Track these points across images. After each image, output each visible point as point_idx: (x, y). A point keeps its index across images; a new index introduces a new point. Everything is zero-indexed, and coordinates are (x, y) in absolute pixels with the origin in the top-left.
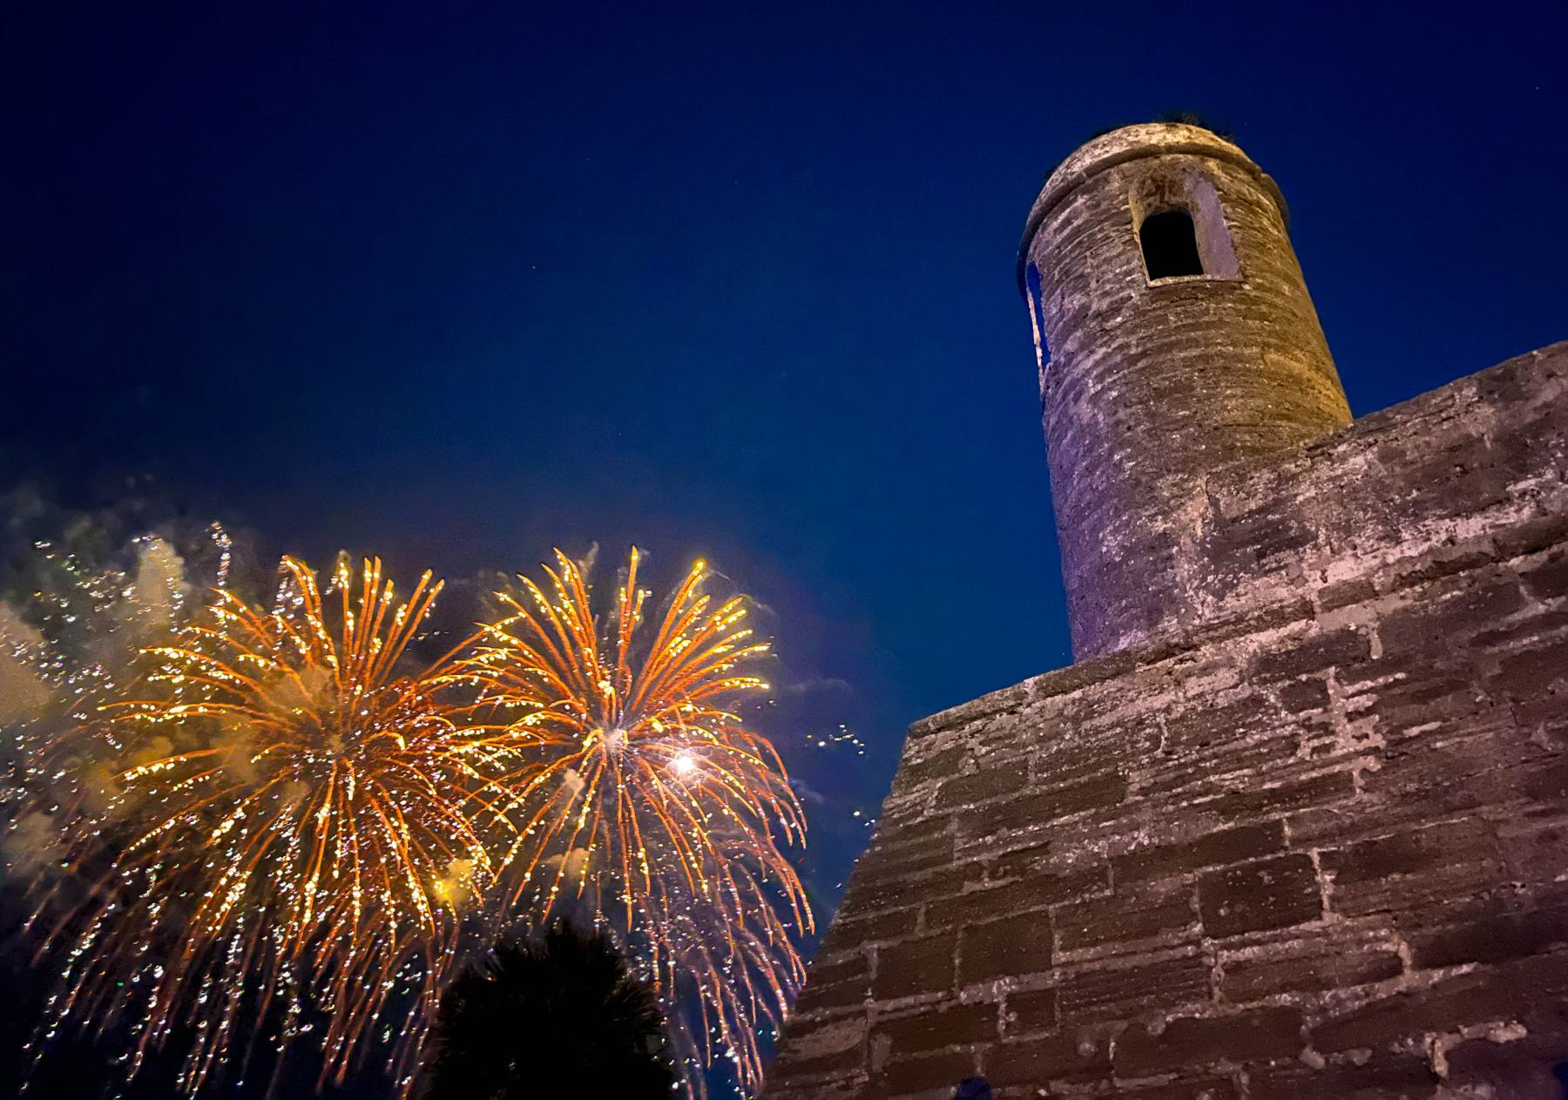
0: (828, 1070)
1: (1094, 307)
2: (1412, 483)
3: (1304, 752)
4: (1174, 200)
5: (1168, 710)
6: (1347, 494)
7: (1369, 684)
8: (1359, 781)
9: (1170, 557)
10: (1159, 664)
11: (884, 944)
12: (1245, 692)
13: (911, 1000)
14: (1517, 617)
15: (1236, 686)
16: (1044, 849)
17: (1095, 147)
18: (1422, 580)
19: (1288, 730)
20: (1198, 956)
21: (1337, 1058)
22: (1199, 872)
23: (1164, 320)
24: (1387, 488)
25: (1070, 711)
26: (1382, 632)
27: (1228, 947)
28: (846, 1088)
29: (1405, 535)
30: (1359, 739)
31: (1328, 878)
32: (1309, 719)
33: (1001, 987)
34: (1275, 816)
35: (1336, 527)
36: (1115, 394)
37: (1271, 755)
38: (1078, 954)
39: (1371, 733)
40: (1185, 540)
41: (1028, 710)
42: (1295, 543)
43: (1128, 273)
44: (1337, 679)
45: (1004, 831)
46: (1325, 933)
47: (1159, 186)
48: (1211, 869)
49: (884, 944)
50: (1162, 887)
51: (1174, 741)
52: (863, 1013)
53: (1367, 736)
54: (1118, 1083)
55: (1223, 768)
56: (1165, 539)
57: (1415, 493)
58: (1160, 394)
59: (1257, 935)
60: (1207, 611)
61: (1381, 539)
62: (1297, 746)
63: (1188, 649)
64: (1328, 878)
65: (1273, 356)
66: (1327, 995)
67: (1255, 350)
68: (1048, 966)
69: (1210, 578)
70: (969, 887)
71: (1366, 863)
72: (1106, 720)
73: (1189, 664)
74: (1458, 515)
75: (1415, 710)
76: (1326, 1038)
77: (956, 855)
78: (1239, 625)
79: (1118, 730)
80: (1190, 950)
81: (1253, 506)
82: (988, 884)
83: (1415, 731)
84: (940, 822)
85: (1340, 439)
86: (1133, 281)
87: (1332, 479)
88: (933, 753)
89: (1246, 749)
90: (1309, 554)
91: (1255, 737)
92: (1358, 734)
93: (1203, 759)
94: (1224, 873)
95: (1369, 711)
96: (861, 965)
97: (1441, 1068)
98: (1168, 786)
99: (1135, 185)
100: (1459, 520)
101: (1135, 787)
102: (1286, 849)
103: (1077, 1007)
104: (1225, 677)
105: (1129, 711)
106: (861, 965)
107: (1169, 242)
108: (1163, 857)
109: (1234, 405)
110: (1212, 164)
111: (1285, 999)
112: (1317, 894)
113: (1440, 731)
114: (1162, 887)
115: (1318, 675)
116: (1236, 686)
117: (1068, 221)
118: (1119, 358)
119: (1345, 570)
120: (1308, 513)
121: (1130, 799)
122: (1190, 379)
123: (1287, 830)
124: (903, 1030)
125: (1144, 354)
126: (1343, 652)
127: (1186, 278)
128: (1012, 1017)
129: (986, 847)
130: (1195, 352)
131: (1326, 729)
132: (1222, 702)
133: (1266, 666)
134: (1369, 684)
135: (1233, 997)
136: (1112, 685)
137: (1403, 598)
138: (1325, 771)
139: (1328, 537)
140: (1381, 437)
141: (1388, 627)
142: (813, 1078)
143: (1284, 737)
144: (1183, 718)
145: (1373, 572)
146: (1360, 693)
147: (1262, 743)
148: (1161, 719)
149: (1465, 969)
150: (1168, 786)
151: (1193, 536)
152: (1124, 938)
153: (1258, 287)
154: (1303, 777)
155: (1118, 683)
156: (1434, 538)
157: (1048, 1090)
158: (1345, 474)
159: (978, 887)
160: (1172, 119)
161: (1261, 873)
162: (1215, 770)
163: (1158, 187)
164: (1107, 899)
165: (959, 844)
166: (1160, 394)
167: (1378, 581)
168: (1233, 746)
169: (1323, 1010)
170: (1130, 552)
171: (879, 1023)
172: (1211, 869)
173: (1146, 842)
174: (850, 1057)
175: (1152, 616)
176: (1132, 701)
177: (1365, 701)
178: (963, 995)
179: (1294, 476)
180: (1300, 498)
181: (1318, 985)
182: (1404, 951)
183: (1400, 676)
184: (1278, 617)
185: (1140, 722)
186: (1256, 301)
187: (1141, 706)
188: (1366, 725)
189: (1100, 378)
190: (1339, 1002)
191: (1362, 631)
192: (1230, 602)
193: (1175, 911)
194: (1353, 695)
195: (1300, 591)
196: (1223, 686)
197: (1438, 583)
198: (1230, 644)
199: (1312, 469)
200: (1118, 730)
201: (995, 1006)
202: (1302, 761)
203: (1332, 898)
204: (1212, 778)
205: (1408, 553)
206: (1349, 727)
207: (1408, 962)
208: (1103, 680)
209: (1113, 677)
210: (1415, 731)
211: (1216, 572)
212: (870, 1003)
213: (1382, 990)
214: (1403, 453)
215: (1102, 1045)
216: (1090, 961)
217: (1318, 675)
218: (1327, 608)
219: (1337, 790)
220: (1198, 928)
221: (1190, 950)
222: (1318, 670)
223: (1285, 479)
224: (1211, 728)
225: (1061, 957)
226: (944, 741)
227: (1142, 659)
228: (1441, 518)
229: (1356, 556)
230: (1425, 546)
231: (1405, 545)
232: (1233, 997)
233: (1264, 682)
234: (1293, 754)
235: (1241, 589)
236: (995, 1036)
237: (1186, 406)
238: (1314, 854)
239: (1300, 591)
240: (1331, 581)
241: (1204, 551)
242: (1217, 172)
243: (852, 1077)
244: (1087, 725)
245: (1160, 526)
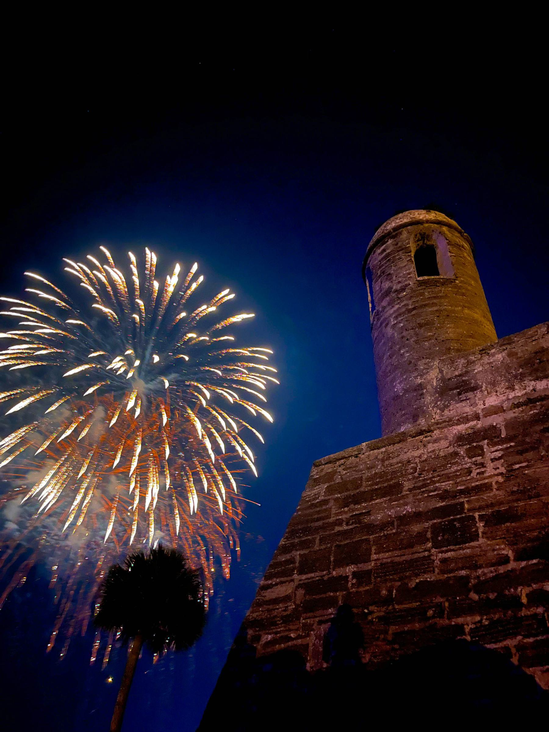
0: (278, 604)
1: (394, 288)
2: (521, 366)
3: (474, 474)
4: (428, 243)
5: (420, 457)
6: (495, 369)
7: (500, 447)
8: (495, 486)
9: (422, 394)
10: (417, 438)
11: (302, 552)
12: (451, 450)
13: (312, 575)
15: (448, 447)
16: (368, 513)
17: (397, 219)
18: (522, 406)
20: (429, 556)
21: (483, 596)
22: (431, 522)
23: (422, 294)
24: (510, 368)
25: (380, 457)
26: (506, 426)
27: (442, 552)
28: (285, 611)
29: (516, 387)
30: (496, 469)
31: (481, 525)
32: (476, 461)
33: (350, 569)
34: (461, 500)
35: (490, 383)
36: (402, 325)
38: (381, 555)
39: (500, 467)
40: (429, 387)
41: (363, 456)
42: (474, 389)
43: (409, 274)
44: (488, 445)
45: (352, 506)
46: (480, 546)
47: (424, 236)
48: (435, 521)
49: (302, 552)
50: (416, 528)
51: (422, 470)
52: (292, 580)
53: (498, 468)
54: (397, 607)
55: (442, 481)
56: (421, 386)
57: (521, 370)
58: (421, 326)
59: (452, 547)
60: (437, 416)
61: (507, 388)
62: (471, 472)
63: (429, 432)
64: (481, 525)
65: (466, 311)
66: (480, 571)
67: (460, 308)
68: (369, 560)
69: (439, 403)
70: (337, 529)
71: (495, 520)
72: (395, 461)
73: (429, 438)
74: (537, 380)
75: (518, 458)
76: (478, 589)
77: (332, 516)
78: (450, 422)
79: (400, 465)
80: (426, 554)
81: (457, 373)
82: (345, 528)
83: (517, 466)
85: (492, 347)
86: (411, 277)
87: (488, 363)
88: (323, 473)
89: (451, 473)
90: (479, 394)
91: (454, 468)
92: (495, 467)
93: (434, 477)
94: (441, 522)
95: (500, 458)
96: (292, 561)
97: (524, 600)
98: (419, 488)
99: (413, 236)
100: (538, 382)
101: (406, 488)
102: (465, 513)
103: (380, 577)
104: (444, 443)
105: (404, 457)
106: (292, 561)
107: (426, 261)
108: (418, 516)
109: (451, 331)
110: (445, 229)
111: (463, 573)
112: (477, 531)
113: (527, 466)
114: (416, 528)
115: (480, 443)
116: (448, 447)
117: (384, 250)
118: (404, 310)
119: (492, 401)
120: (478, 376)
121: (404, 493)
122: (433, 320)
123: (466, 506)
124: (308, 587)
125: (414, 309)
126: (490, 434)
127: (433, 277)
128: (354, 581)
129: (346, 513)
130: (435, 308)
131: (483, 465)
132: (442, 454)
133: (461, 439)
134: (500, 447)
135: (442, 572)
136: (397, 446)
137: (514, 413)
138: (481, 482)
139: (486, 387)
140: (509, 347)
141: (509, 425)
142: (271, 607)
143: (466, 468)
144: (426, 460)
145: (503, 401)
146: (496, 451)
147: (457, 471)
148: (417, 460)
149: (535, 561)
150: (419, 488)
151: (432, 385)
152: (400, 549)
153: (461, 282)
154: (473, 484)
155: (400, 445)
156: (528, 388)
157: (368, 610)
158: (494, 362)
159: (340, 529)
160: (428, 208)
161: (455, 523)
162: (438, 481)
163: (422, 238)
164: (394, 534)
165: (334, 511)
166: (421, 326)
167: (505, 406)
168: (446, 472)
169: (478, 577)
170: (406, 391)
171: (299, 584)
172: (435, 521)
173: (410, 510)
174: (287, 599)
175: (415, 418)
176: (405, 453)
177: (499, 454)
178: (334, 573)
179: (474, 362)
180: (476, 371)
181: (476, 567)
182: (510, 554)
183: (512, 444)
184: (466, 420)
185: (409, 462)
186: (460, 288)
187: (410, 454)
188: (498, 464)
189: (396, 318)
190: (485, 574)
191: (498, 426)
192: (446, 412)
193: (421, 538)
194: (494, 452)
195: (475, 409)
196: (443, 447)
197: (528, 407)
198: (446, 430)
199: (481, 359)
200: (400, 465)
201: (348, 577)
202: (473, 478)
203: (483, 533)
204: (437, 485)
205: (517, 395)
206: (492, 464)
207: (512, 558)
208: (394, 444)
209: (398, 443)
210: (517, 466)
211: (441, 400)
212: (296, 576)
213: (502, 570)
214: (517, 354)
215: (390, 591)
216: (387, 558)
217: (480, 443)
218: (485, 416)
219: (486, 490)
220: (430, 545)
221: (426, 554)
222: (480, 441)
223: (470, 363)
224: (438, 465)
225: (374, 557)
226: (328, 468)
227: (410, 436)
228: (531, 381)
229: (497, 395)
230: (524, 392)
231: (516, 391)
232: (442, 572)
233: (460, 445)
234: (469, 475)
235: (451, 408)
236: (347, 589)
237: (430, 331)
238: (477, 515)
239: (475, 409)
240: (487, 405)
241: (436, 392)
242: (447, 232)
243: (287, 607)
244: (387, 462)
245: (419, 381)
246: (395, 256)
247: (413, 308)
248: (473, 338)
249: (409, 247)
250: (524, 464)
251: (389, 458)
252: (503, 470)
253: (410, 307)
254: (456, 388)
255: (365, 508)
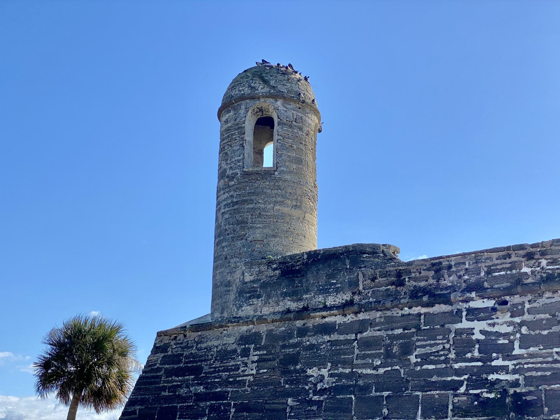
3: (240, 371)
5: (217, 347)
11: (141, 407)
12: (234, 346)
14: (291, 341)
15: (233, 344)
19: (239, 363)
26: (267, 335)
37: (234, 370)
45: (174, 378)
49: (141, 407)
56: (228, 284)
58: (238, 223)
65: (277, 207)
72: (204, 346)
82: (167, 394)
84: (159, 370)
94: (215, 404)
95: (256, 362)
105: (210, 344)
115: (250, 346)
116: (233, 344)
118: (230, 201)
130: (251, 206)
131: (246, 364)
141: (270, 333)
144: (220, 351)
147: (233, 365)
151: (236, 284)
163: (260, 110)
166: (238, 223)
167: (269, 319)
168: (227, 364)
177: (256, 358)
228: (289, 300)
246: (232, 135)
247: (236, 202)
248: (276, 237)
249: (244, 127)
250: (265, 371)
251: (201, 342)
252: (254, 372)
253: (235, 200)
254: (249, 293)
255: (180, 381)
